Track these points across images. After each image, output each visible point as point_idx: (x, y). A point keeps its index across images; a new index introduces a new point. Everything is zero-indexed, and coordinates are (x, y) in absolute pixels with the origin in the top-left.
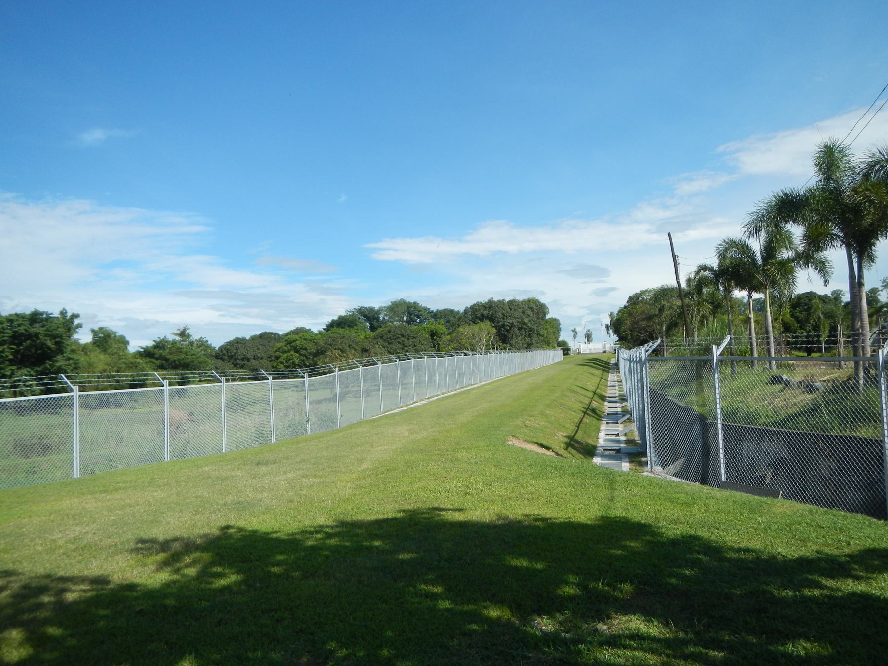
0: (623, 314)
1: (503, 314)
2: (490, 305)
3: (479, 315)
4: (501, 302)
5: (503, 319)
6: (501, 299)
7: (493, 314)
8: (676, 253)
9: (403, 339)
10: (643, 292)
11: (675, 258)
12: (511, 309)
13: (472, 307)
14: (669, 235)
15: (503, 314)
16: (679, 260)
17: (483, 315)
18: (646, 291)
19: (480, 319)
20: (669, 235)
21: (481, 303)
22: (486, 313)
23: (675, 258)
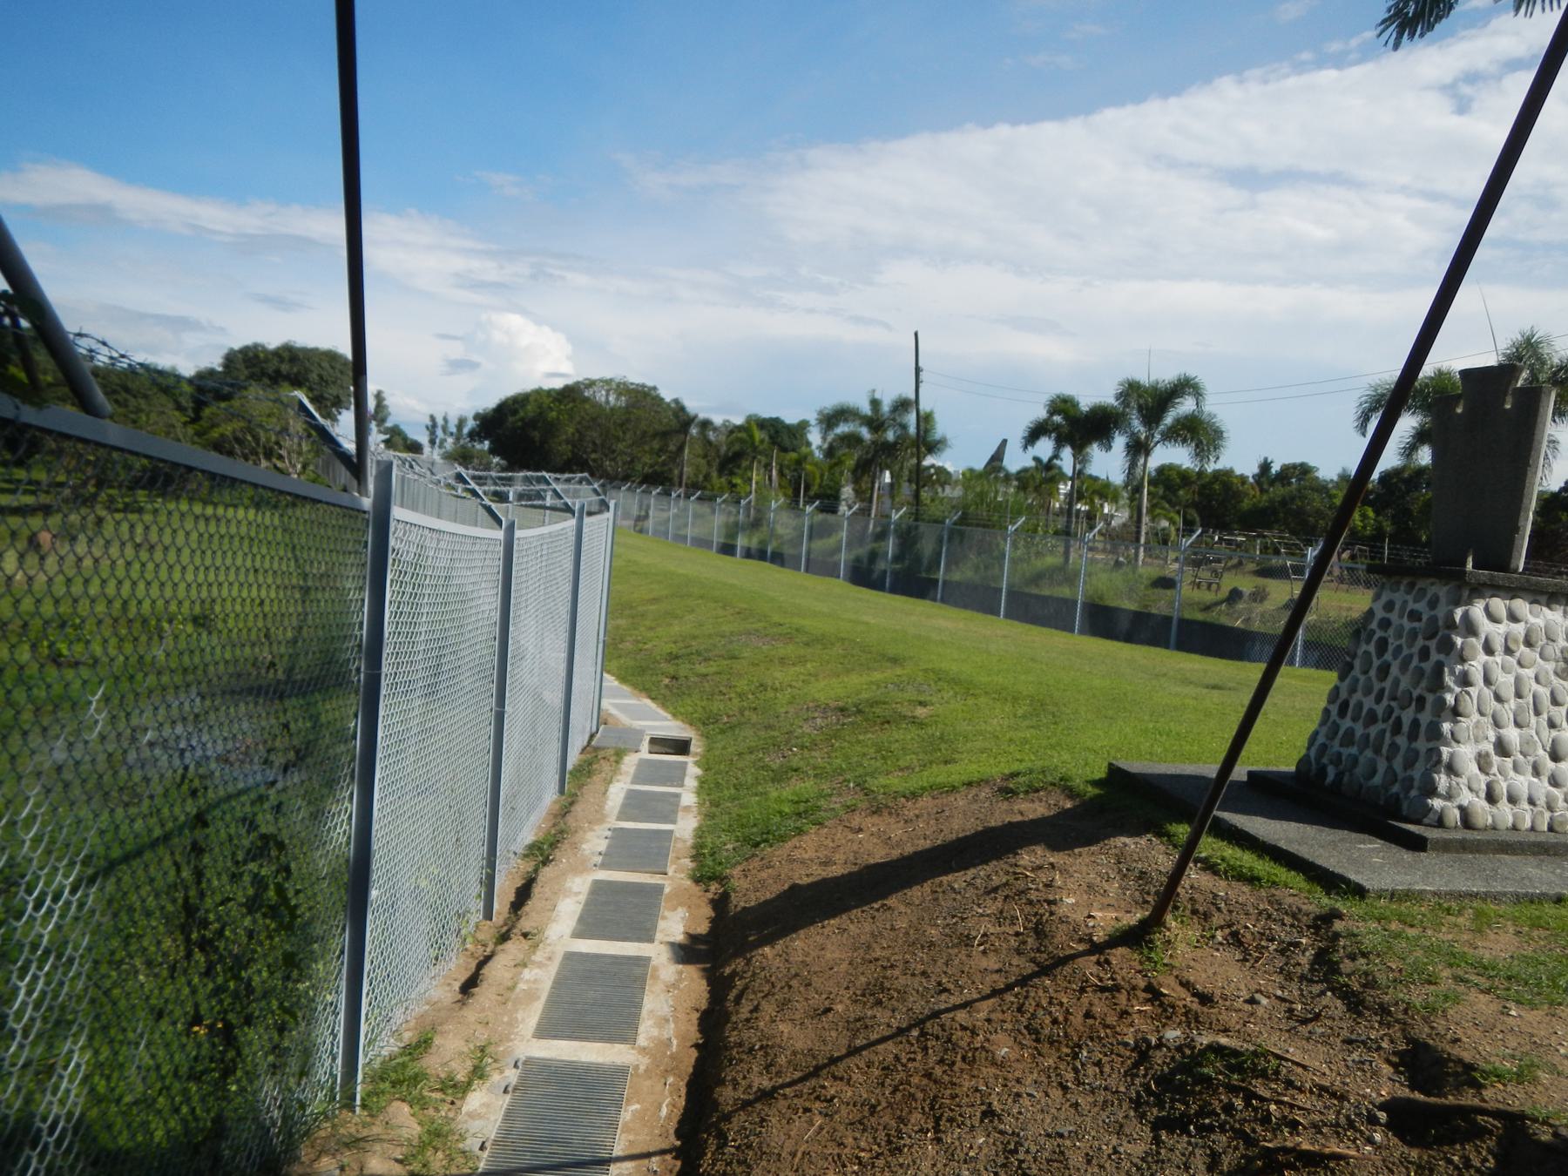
0: (560, 412)
1: (321, 377)
2: (289, 354)
3: (270, 371)
4: (315, 351)
5: (320, 384)
6: (650, 383)
7: (299, 372)
8: (920, 364)
9: (124, 395)
10: (591, 384)
11: (918, 370)
12: (332, 368)
13: (245, 351)
14: (916, 334)
15: (321, 377)
16: (923, 376)
17: (278, 372)
18: (601, 380)
19: (270, 378)
20: (916, 334)
21: (263, 347)
22: (285, 368)
23: (918, 370)
